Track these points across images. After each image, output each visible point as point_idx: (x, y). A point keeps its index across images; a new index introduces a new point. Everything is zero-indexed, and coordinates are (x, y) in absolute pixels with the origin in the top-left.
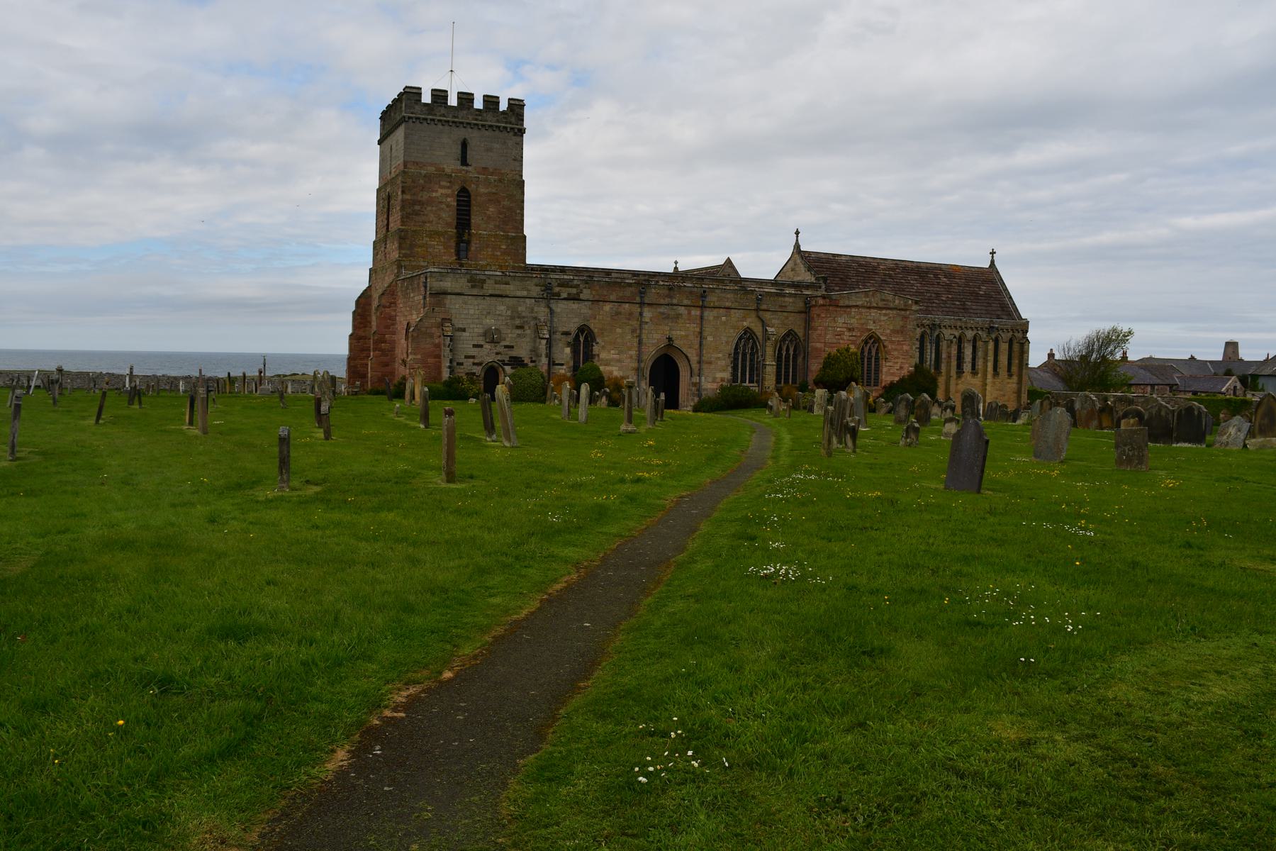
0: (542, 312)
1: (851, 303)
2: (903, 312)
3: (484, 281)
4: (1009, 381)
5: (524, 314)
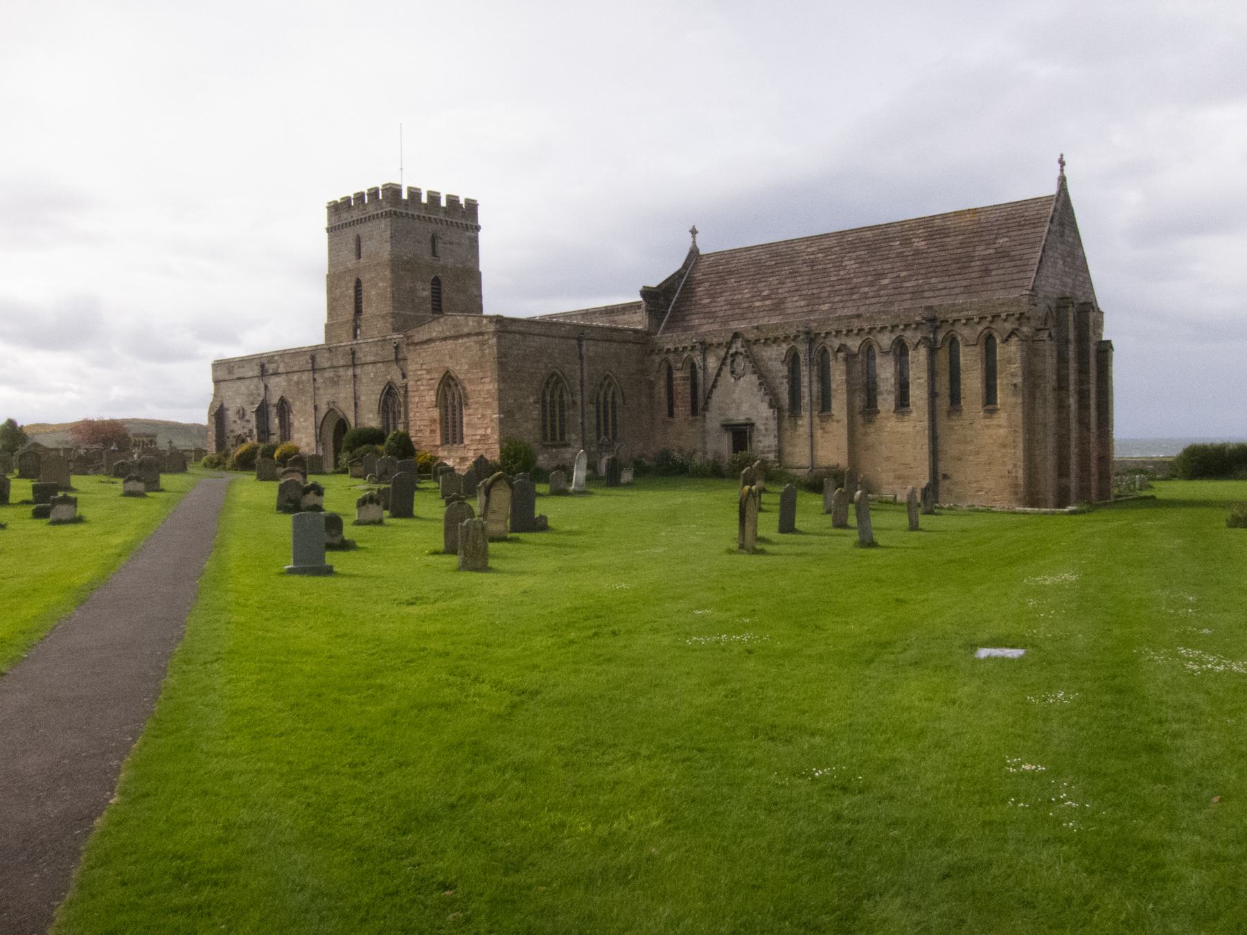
1: (426, 337)
2: (481, 337)
4: (987, 422)
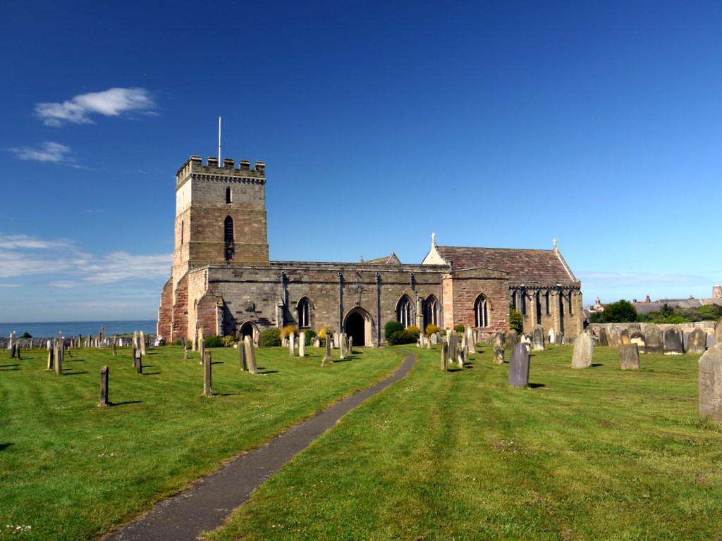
0: (280, 288)
3: (242, 273)
5: (267, 292)
